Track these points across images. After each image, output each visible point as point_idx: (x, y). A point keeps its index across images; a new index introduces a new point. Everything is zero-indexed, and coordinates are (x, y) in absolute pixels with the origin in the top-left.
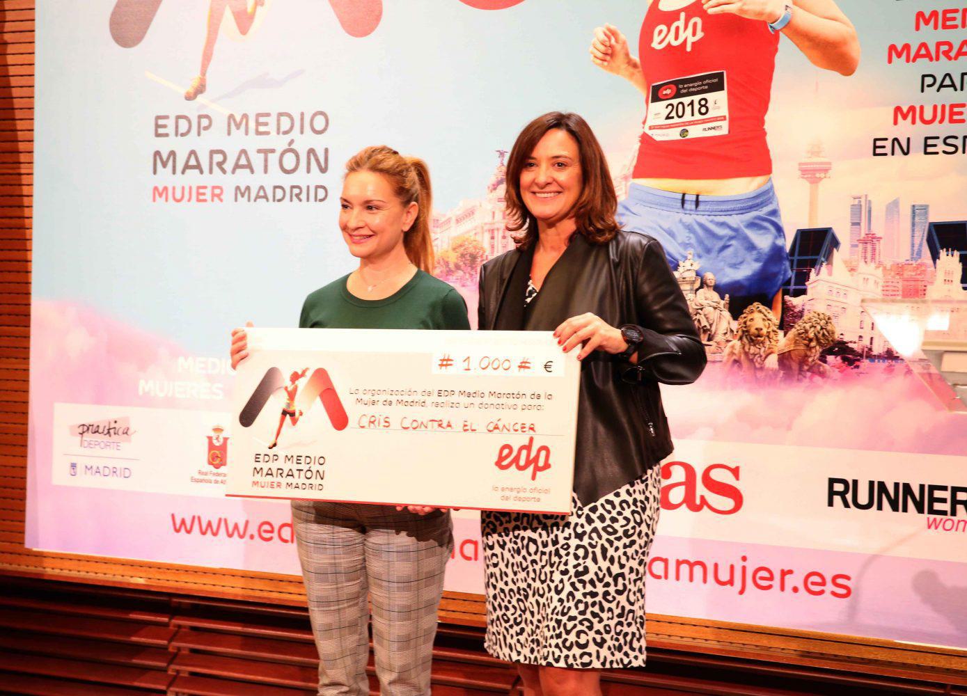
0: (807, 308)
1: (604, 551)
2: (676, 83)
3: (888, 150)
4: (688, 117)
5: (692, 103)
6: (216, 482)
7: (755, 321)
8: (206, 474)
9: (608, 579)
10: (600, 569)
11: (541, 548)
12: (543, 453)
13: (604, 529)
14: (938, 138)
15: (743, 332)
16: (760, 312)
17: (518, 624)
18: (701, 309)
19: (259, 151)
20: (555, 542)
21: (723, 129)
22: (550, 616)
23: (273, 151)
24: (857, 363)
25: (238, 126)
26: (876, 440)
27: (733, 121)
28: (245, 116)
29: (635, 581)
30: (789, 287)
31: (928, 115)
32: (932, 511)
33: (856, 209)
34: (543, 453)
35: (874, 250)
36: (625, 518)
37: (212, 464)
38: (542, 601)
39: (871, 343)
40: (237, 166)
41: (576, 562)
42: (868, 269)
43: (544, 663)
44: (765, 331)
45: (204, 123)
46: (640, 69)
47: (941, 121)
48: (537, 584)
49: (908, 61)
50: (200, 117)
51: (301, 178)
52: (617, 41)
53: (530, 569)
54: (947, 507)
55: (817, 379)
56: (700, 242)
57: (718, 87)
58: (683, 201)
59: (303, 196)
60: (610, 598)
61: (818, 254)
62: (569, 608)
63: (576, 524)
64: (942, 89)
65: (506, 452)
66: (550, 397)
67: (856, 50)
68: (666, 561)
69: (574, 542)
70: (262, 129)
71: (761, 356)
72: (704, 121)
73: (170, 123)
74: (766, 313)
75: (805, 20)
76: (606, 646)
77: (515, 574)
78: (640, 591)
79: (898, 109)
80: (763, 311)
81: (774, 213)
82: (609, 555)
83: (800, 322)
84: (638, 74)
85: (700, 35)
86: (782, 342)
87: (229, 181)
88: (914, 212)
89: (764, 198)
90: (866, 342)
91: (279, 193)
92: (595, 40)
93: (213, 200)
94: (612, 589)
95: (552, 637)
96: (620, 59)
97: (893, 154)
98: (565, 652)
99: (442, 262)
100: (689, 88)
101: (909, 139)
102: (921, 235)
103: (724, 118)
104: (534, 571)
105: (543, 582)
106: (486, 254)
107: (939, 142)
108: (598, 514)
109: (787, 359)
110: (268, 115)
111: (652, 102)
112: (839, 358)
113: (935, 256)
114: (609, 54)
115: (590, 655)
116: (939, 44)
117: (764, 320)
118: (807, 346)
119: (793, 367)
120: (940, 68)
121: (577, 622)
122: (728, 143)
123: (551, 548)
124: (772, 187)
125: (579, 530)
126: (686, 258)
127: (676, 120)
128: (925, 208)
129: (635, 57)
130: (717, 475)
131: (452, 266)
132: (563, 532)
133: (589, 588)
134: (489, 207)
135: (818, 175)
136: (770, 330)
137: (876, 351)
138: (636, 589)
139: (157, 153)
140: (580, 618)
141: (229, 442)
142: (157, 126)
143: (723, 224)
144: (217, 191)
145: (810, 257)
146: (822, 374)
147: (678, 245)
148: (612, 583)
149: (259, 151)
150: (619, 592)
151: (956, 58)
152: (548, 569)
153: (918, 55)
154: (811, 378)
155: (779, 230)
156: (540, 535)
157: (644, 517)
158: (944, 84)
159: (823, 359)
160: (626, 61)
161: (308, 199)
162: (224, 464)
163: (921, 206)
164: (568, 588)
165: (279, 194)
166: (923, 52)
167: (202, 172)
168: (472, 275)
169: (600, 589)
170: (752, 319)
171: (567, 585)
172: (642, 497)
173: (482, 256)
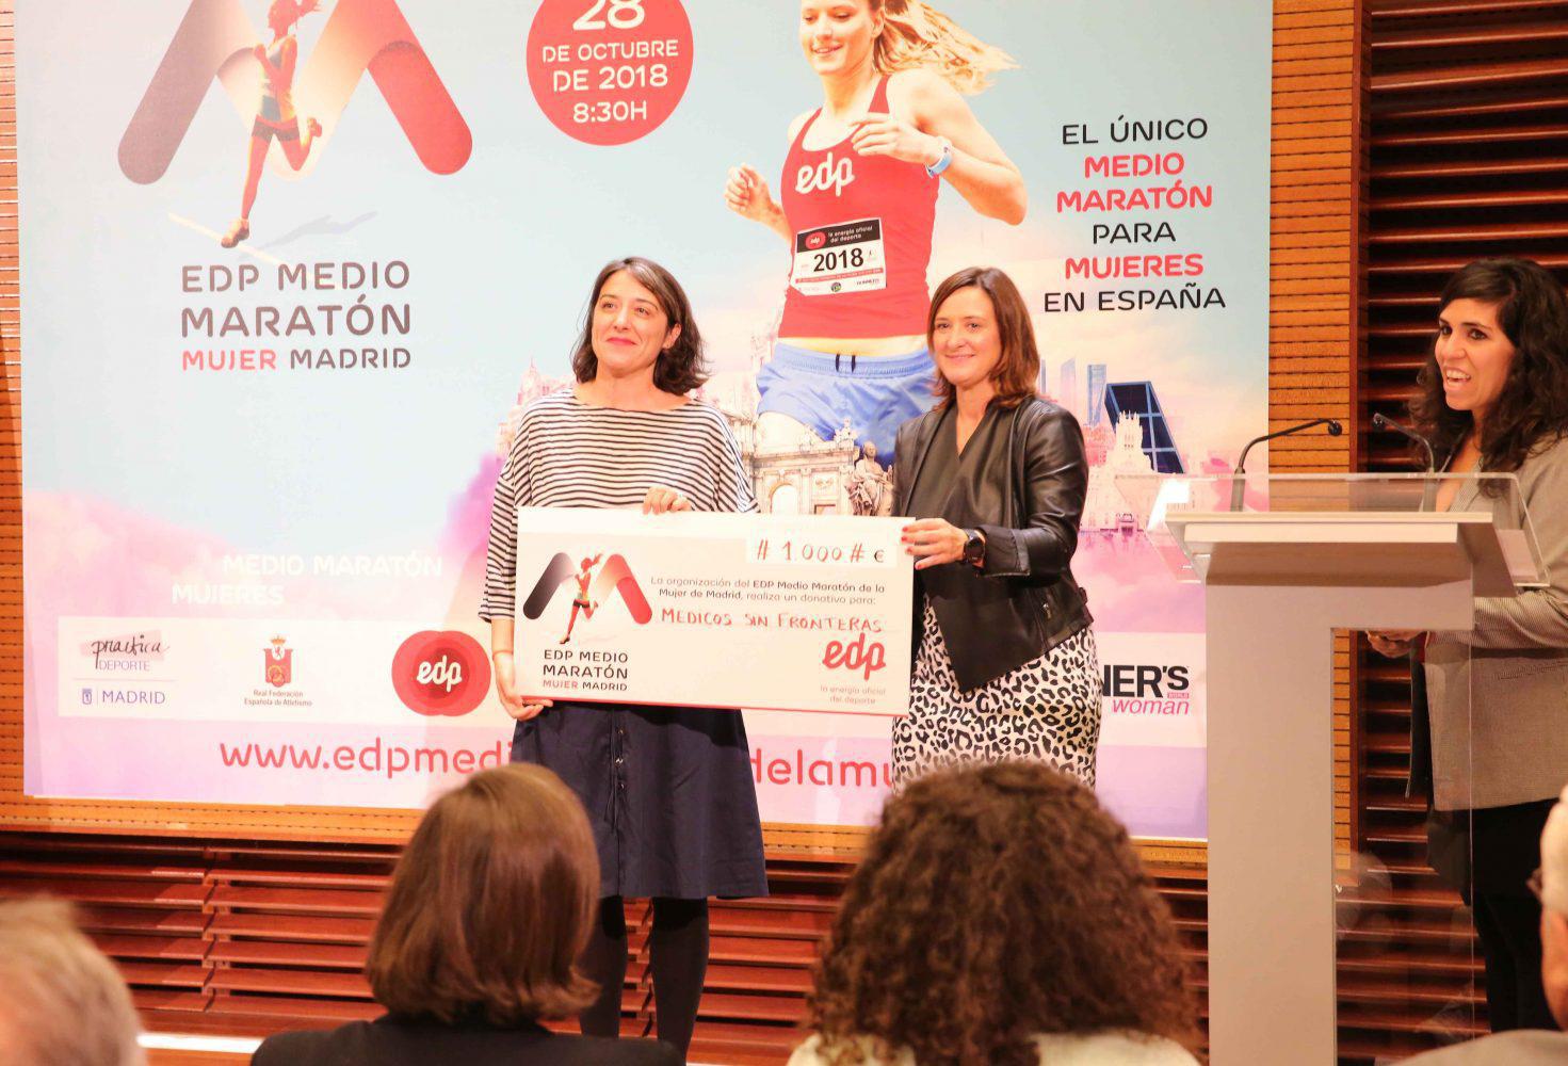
1: (1047, 743)
2: (826, 231)
3: (1061, 305)
4: (840, 269)
5: (844, 253)
13: (1044, 720)
20: (992, 736)
21: (880, 282)
23: (339, 308)
25: (292, 279)
28: (302, 267)
31: (1102, 269)
40: (292, 326)
45: (248, 274)
47: (1116, 274)
49: (1078, 209)
51: (375, 339)
52: (755, 183)
56: (859, 408)
57: (874, 236)
59: (380, 361)
69: (1013, 736)
70: (323, 282)
72: (858, 274)
73: (204, 275)
75: (967, 163)
79: (1070, 262)
82: (1052, 747)
84: (781, 221)
85: (850, 178)
87: (283, 345)
88: (1090, 372)
91: (348, 358)
92: (729, 182)
93: (262, 367)
97: (1066, 309)
100: (840, 237)
101: (1082, 294)
102: (1099, 397)
103: (881, 270)
107: (1115, 298)
113: (1114, 420)
114: (747, 197)
116: (1110, 193)
120: (1112, 218)
125: (1018, 723)
126: (843, 426)
127: (827, 272)
128: (1102, 368)
129: (777, 201)
132: (1001, 725)
139: (187, 312)
142: (186, 279)
144: (268, 356)
147: (833, 413)
151: (1129, 208)
153: (1088, 204)
156: (973, 729)
158: (1118, 235)
161: (385, 365)
163: (1098, 366)
165: (347, 359)
166: (1094, 200)
167: (246, 333)
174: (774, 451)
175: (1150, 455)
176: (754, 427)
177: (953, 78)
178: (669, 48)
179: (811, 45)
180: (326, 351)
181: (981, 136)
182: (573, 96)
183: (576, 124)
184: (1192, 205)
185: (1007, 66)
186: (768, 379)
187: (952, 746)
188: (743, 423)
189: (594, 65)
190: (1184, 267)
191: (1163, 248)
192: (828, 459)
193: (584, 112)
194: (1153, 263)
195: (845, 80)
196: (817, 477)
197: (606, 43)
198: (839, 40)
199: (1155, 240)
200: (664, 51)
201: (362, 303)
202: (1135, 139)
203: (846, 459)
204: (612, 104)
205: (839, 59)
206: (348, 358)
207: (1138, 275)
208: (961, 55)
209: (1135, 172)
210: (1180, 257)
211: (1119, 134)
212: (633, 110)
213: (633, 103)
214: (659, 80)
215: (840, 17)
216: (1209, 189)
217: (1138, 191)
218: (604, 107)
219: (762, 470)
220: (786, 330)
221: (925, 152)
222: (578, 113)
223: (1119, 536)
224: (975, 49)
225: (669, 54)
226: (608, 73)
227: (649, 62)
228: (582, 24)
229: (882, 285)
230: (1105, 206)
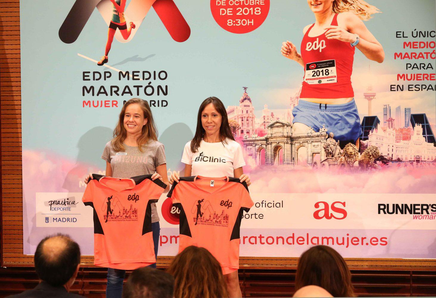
0: (369, 144)
2: (316, 63)
3: (396, 89)
4: (321, 76)
5: (322, 71)
14: (413, 85)
15: (345, 153)
16: (351, 146)
18: (329, 146)
19: (135, 86)
21: (335, 81)
23: (141, 86)
24: (388, 163)
25: (124, 76)
26: (395, 190)
30: (362, 137)
31: (409, 77)
32: (415, 213)
33: (385, 110)
35: (392, 124)
39: (392, 156)
40: (124, 92)
42: (390, 130)
44: (353, 153)
45: (108, 75)
47: (414, 80)
49: (401, 58)
50: (105, 73)
52: (292, 47)
54: (420, 211)
55: (373, 169)
56: (327, 121)
58: (320, 106)
59: (156, 104)
61: (372, 125)
67: (383, 54)
68: (318, 238)
70: (135, 77)
71: (352, 162)
73: (91, 75)
74: (353, 146)
75: (363, 43)
79: (399, 75)
80: (353, 146)
81: (355, 111)
83: (366, 149)
84: (301, 60)
85: (325, 46)
86: (360, 157)
88: (405, 111)
89: (352, 105)
90: (390, 156)
92: (283, 47)
93: (113, 106)
96: (293, 54)
97: (397, 90)
100: (321, 65)
101: (403, 85)
102: (408, 118)
103: (335, 77)
107: (413, 87)
109: (362, 163)
112: (381, 162)
113: (413, 126)
114: (289, 52)
116: (412, 53)
117: (353, 149)
118: (369, 158)
119: (364, 166)
120: (413, 61)
122: (337, 85)
124: (354, 102)
126: (322, 127)
127: (317, 77)
128: (409, 109)
129: (299, 53)
130: (337, 206)
134: (240, 109)
135: (371, 97)
136: (355, 152)
137: (394, 159)
139: (85, 87)
142: (84, 76)
143: (336, 115)
144: (115, 103)
145: (369, 126)
146: (375, 168)
147: (319, 123)
149: (135, 86)
151: (418, 58)
153: (405, 57)
154: (371, 169)
155: (357, 117)
158: (414, 67)
159: (375, 162)
160: (296, 55)
161: (158, 106)
163: (408, 108)
166: (406, 56)
170: (348, 149)
174: (299, 135)
175: (425, 137)
176: (292, 127)
177: (360, 15)
179: (311, 3)
181: (369, 34)
182: (227, 17)
183: (229, 26)
185: (378, 12)
186: (296, 111)
188: (288, 126)
191: (429, 71)
192: (317, 138)
194: (426, 76)
195: (323, 14)
196: (313, 144)
198: (320, 2)
199: (427, 69)
200: (260, 3)
201: (150, 85)
202: (420, 37)
203: (323, 138)
204: (241, 21)
205: (321, 8)
207: (421, 80)
208: (362, 8)
209: (420, 47)
211: (415, 35)
212: (249, 22)
213: (248, 20)
214: (258, 12)
217: (421, 53)
218: (238, 21)
219: (294, 142)
220: (302, 96)
221: (350, 38)
223: (415, 163)
224: (367, 6)
225: (261, 4)
226: (240, 10)
229: (335, 81)
230: (410, 58)
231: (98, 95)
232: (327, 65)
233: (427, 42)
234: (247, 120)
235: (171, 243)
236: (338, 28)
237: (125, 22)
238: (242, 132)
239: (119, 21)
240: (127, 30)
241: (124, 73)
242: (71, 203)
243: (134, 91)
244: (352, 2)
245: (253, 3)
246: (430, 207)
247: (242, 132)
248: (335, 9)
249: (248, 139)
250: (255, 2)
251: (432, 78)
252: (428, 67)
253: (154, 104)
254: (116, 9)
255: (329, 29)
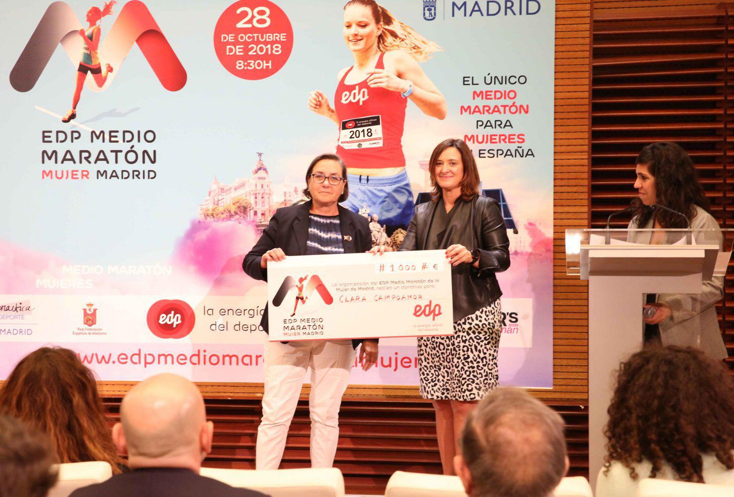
1: (476, 347)
2: (355, 121)
4: (361, 137)
5: (363, 131)
6: (90, 334)
7: (399, 237)
8: (83, 330)
9: (478, 360)
10: (474, 355)
11: (446, 347)
12: (437, 307)
13: (475, 337)
15: (393, 243)
16: (402, 233)
17: (433, 382)
19: (112, 151)
20: (453, 344)
21: (380, 144)
22: (454, 378)
23: (121, 151)
25: (98, 138)
27: (385, 140)
28: (102, 132)
29: (492, 360)
31: (480, 139)
34: (437, 307)
36: (485, 332)
37: (87, 324)
38: (449, 371)
40: (98, 159)
41: (463, 353)
43: (454, 399)
45: (76, 135)
46: (336, 113)
47: (487, 142)
48: (446, 363)
49: (470, 113)
50: (73, 132)
51: (139, 166)
52: (322, 98)
53: (441, 356)
56: (370, 199)
57: (377, 123)
58: (360, 179)
59: (141, 176)
60: (480, 368)
62: (462, 374)
63: (462, 336)
64: (486, 127)
65: (418, 308)
66: (437, 281)
67: (445, 108)
69: (462, 344)
70: (113, 139)
75: (419, 92)
76: (482, 389)
77: (433, 359)
78: (495, 364)
82: (478, 349)
84: (335, 116)
85: (366, 97)
87: (93, 168)
89: (403, 177)
91: (125, 174)
92: (310, 98)
93: (82, 178)
94: (481, 364)
95: (457, 387)
98: (463, 394)
99: (226, 211)
100: (362, 123)
104: (443, 357)
105: (449, 363)
106: (252, 206)
107: (486, 152)
108: (472, 331)
110: (117, 132)
111: (343, 129)
114: (318, 105)
115: (474, 394)
116: (484, 107)
120: (485, 117)
121: (466, 380)
123: (451, 347)
124: (406, 172)
125: (464, 339)
126: (362, 207)
127: (356, 139)
129: (333, 107)
131: (233, 213)
132: (456, 339)
133: (471, 365)
134: (254, 182)
138: (493, 363)
139: (44, 152)
140: (468, 378)
141: (97, 311)
142: (44, 137)
143: (381, 191)
144: (85, 173)
148: (481, 362)
149: (112, 151)
150: (484, 365)
151: (492, 113)
152: (450, 356)
153: (474, 112)
155: (410, 193)
157: (494, 330)
158: (487, 125)
161: (144, 178)
162: (95, 324)
164: (461, 365)
165: (125, 175)
166: (477, 110)
167: (75, 162)
168: (245, 217)
169: (475, 365)
170: (397, 237)
171: (461, 364)
172: (493, 321)
173: (250, 207)
178: (282, 37)
179: (348, 38)
180: (114, 171)
181: (426, 80)
182: (237, 57)
183: (239, 70)
184: (520, 112)
185: (438, 50)
187: (437, 349)
189: (246, 44)
190: (516, 139)
191: (507, 131)
193: (242, 65)
194: (503, 137)
195: (365, 53)
197: (252, 34)
199: (504, 128)
200: (280, 38)
201: (133, 149)
202: (495, 84)
204: (255, 62)
205: (361, 45)
206: (125, 174)
207: (496, 143)
208: (416, 44)
209: (495, 98)
210: (515, 135)
211: (488, 81)
213: (264, 62)
214: (277, 51)
215: (362, 26)
216: (528, 106)
217: (496, 106)
218: (251, 63)
222: (238, 65)
224: (424, 42)
226: (252, 48)
227: (272, 43)
228: (240, 25)
231: (62, 162)
232: (370, 122)
233: (505, 92)
234: (262, 198)
235: (159, 363)
236: (384, 72)
237: (99, 64)
238: (255, 213)
239: (91, 61)
240: (101, 76)
241: (98, 134)
242: (24, 309)
243: (111, 157)
244: (403, 37)
245: (270, 39)
246: (508, 317)
247: (255, 213)
248: (381, 46)
249: (263, 223)
250: (273, 37)
251: (511, 141)
252: (505, 126)
253: (137, 176)
254: (86, 46)
255: (372, 74)
